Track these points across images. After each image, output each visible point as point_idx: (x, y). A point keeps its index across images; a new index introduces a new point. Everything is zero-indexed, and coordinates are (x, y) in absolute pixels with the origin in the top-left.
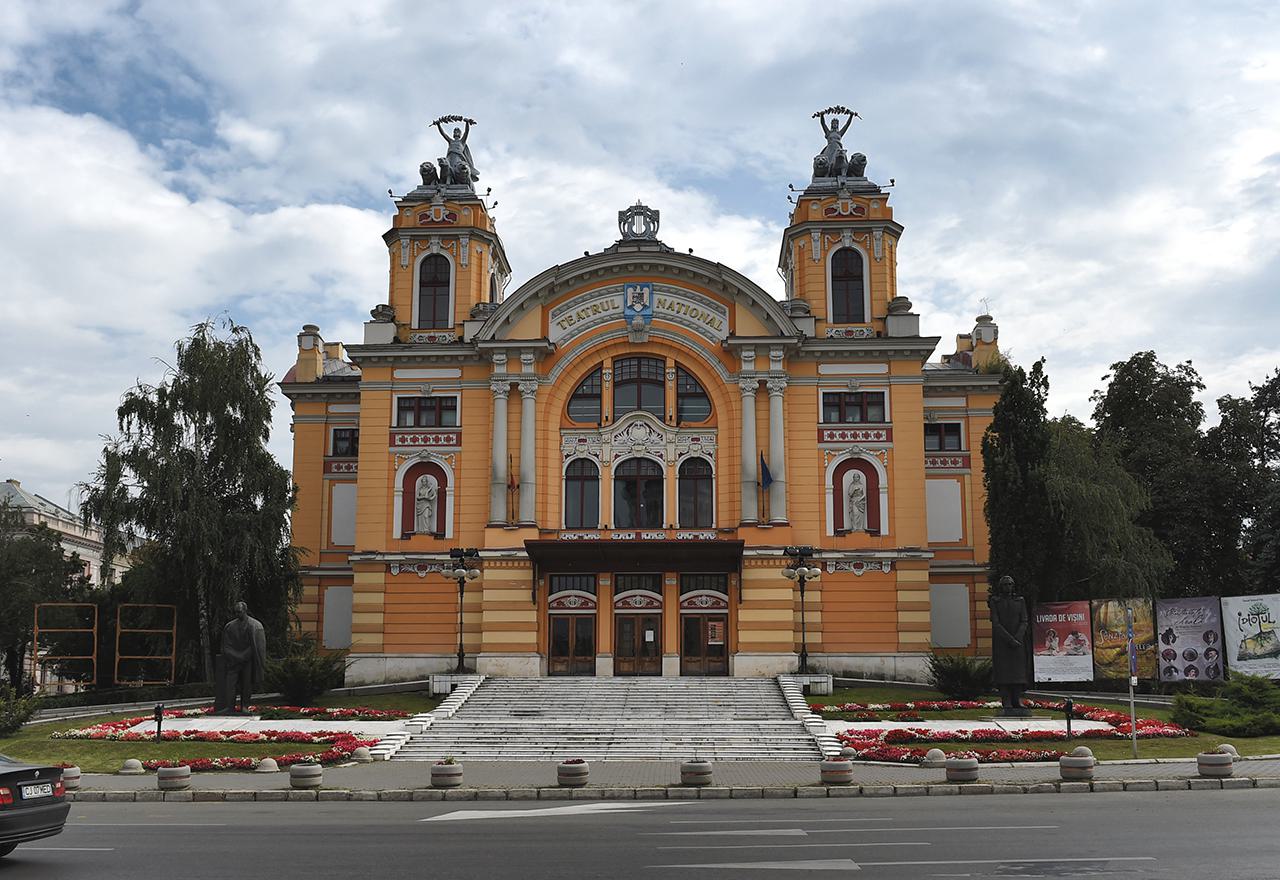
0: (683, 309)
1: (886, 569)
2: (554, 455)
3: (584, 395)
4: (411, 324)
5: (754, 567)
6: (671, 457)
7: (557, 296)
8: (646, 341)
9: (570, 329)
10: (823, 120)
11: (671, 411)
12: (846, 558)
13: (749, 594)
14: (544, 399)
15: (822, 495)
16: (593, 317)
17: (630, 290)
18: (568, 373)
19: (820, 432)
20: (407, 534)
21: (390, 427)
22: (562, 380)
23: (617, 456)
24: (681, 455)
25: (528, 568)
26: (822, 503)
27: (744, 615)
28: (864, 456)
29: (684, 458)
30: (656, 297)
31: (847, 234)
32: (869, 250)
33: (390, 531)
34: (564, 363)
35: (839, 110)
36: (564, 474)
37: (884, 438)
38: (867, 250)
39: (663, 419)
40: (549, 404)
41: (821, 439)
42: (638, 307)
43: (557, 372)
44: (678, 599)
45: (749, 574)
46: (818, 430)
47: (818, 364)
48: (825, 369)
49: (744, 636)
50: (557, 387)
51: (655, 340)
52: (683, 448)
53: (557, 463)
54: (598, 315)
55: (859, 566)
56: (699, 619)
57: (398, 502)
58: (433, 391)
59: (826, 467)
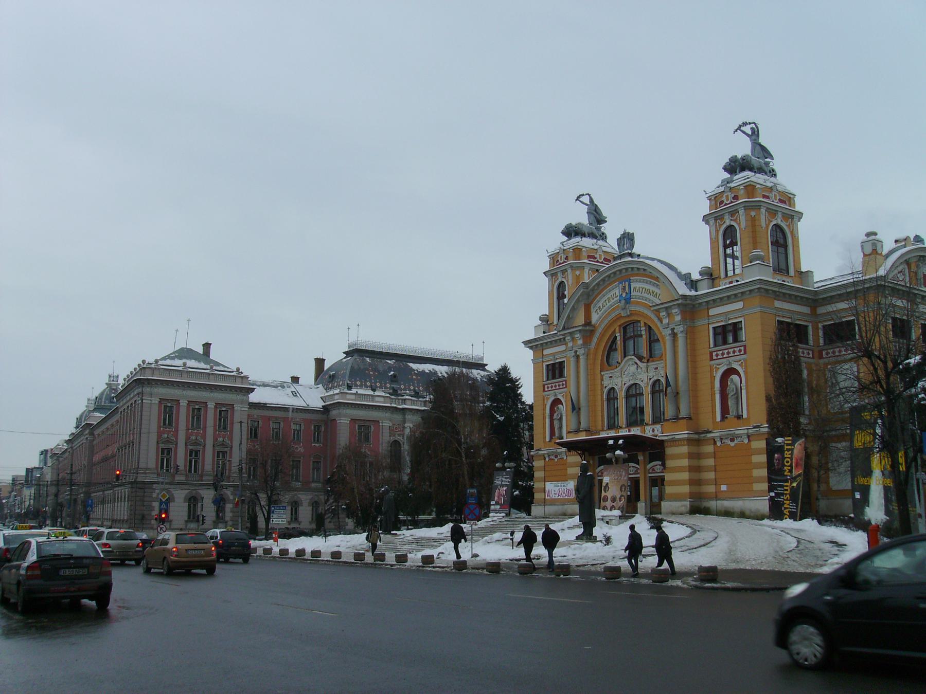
0: (644, 290)
1: (746, 441)
2: (599, 387)
3: (611, 348)
4: (553, 323)
5: (671, 446)
6: (645, 380)
7: (592, 298)
8: (629, 314)
9: (600, 313)
10: (744, 132)
11: (644, 352)
12: (725, 435)
13: (670, 463)
14: (591, 357)
15: (713, 395)
16: (608, 304)
17: (621, 285)
18: (600, 340)
19: (711, 353)
20: (551, 438)
21: (543, 381)
22: (598, 344)
23: (625, 384)
24: (650, 379)
25: (576, 455)
26: (713, 400)
27: (668, 477)
28: (734, 366)
29: (652, 380)
30: (633, 285)
31: (727, 217)
32: (739, 224)
33: (545, 438)
34: (597, 335)
35: (745, 124)
36: (605, 397)
37: (743, 352)
38: (737, 223)
39: (641, 358)
40: (595, 359)
41: (711, 359)
42: (624, 295)
43: (595, 340)
44: (645, 468)
45: (669, 451)
46: (710, 352)
47: (708, 309)
48: (712, 312)
49: (668, 490)
50: (597, 349)
51: (634, 312)
52: (651, 374)
53: (599, 392)
54: (610, 303)
55: (732, 440)
56: (657, 479)
57: (548, 421)
58: (556, 359)
59: (715, 377)
